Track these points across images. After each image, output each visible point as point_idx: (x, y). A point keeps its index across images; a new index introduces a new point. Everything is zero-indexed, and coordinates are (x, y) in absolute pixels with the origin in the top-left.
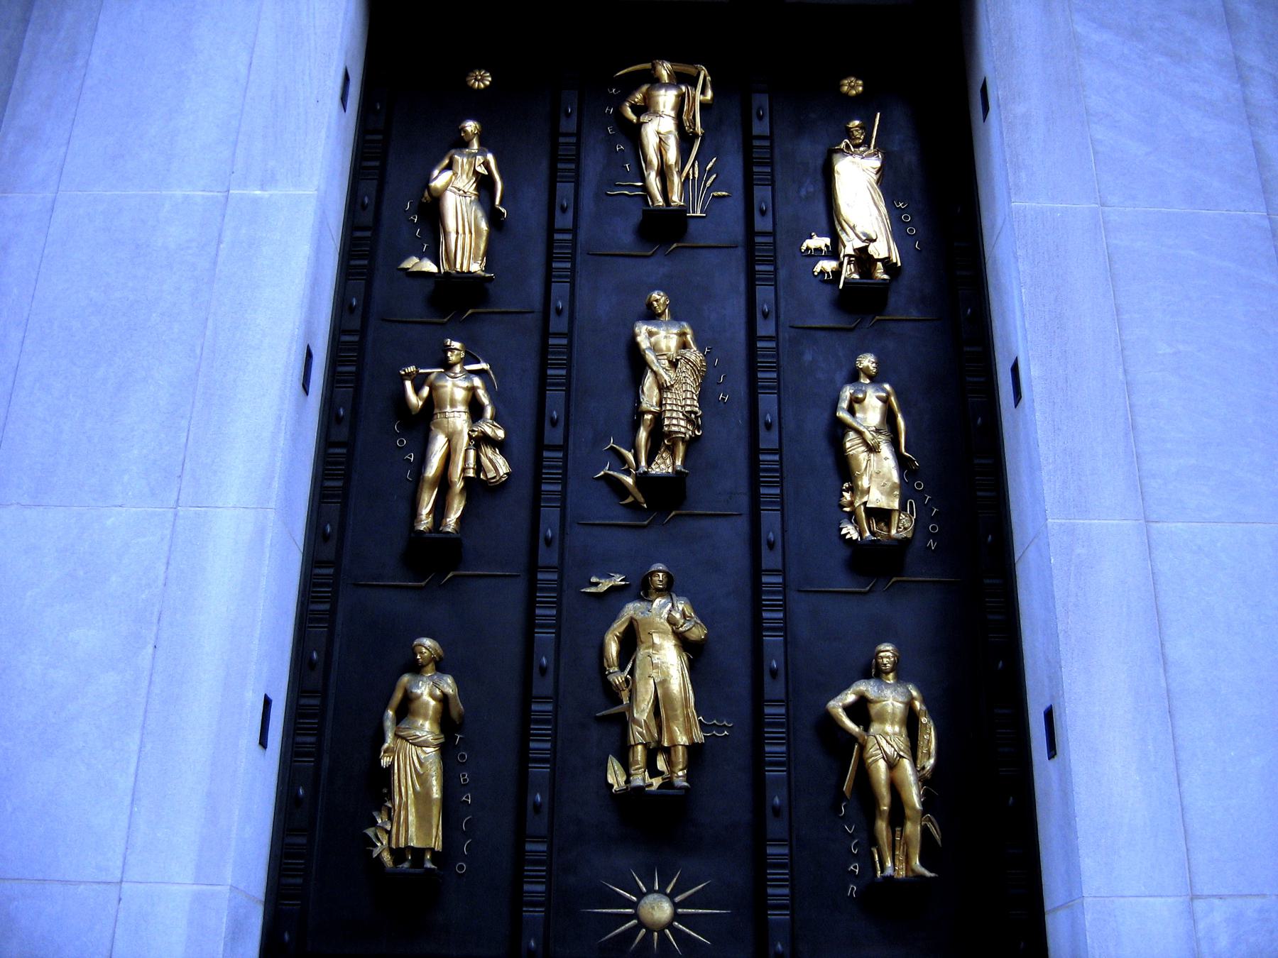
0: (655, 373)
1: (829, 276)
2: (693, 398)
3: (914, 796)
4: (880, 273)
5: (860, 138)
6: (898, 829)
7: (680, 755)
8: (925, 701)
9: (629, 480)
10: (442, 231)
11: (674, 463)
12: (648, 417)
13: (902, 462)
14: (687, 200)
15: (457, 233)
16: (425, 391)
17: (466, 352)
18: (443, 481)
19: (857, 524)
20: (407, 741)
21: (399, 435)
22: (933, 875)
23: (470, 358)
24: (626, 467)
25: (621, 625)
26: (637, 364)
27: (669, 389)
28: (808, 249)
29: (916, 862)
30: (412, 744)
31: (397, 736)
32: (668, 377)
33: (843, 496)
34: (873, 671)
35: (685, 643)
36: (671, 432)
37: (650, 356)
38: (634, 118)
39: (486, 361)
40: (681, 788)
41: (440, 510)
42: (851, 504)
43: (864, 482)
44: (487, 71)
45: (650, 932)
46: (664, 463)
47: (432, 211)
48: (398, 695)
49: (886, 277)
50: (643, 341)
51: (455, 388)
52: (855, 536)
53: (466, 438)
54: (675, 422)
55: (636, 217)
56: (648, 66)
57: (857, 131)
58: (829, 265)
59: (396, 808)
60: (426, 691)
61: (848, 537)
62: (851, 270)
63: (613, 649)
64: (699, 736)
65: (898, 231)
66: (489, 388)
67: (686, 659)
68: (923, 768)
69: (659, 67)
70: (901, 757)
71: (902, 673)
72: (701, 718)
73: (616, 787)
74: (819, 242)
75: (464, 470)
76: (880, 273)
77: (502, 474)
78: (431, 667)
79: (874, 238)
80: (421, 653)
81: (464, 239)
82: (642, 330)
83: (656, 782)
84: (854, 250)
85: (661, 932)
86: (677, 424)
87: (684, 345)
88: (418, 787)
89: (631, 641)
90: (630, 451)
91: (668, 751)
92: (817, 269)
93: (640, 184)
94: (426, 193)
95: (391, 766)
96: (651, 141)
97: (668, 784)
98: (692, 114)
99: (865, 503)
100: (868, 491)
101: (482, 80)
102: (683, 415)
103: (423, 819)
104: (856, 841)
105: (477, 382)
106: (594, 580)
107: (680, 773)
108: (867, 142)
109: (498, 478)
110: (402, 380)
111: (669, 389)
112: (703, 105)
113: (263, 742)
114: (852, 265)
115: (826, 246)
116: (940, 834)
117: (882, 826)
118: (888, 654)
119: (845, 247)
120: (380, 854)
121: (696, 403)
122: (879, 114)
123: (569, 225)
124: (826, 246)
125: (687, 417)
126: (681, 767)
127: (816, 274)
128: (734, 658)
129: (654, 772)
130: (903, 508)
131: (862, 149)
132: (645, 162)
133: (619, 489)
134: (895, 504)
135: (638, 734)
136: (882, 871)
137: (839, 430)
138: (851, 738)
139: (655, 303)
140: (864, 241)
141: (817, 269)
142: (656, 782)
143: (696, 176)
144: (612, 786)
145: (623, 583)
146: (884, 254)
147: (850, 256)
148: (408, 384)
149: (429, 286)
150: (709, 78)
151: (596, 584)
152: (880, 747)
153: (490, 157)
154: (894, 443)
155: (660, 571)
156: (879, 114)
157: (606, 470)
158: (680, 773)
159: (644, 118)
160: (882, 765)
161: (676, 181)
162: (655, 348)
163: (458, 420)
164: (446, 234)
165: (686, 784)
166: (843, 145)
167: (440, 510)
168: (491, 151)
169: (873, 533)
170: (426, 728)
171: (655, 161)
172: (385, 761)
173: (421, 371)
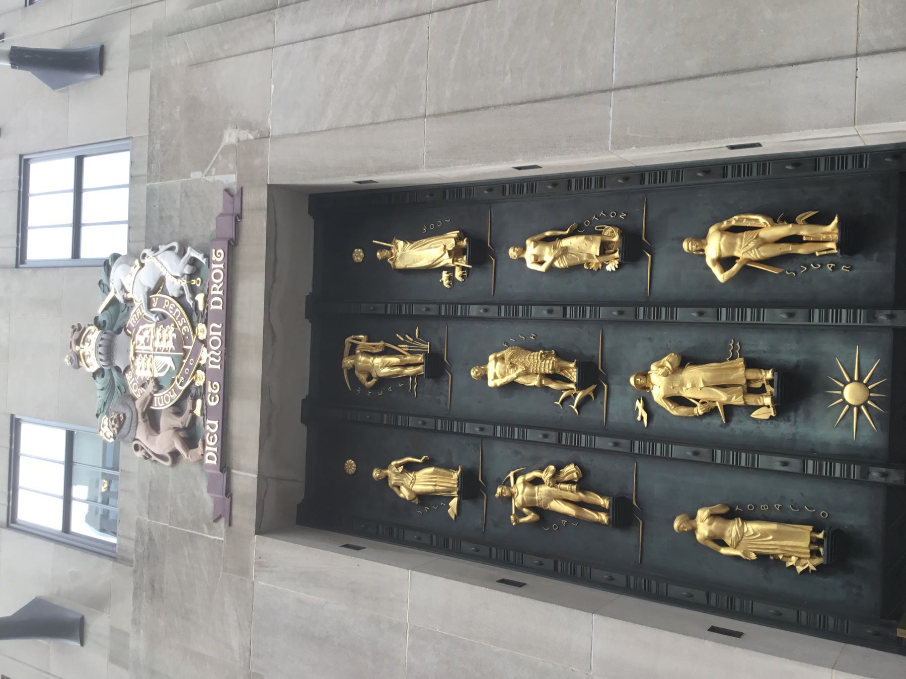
1: (465, 273)
2: (533, 355)
3: (783, 230)
5: (387, 253)
6: (804, 239)
7: (752, 374)
10: (434, 494)
13: (573, 234)
14: (420, 353)
15: (435, 485)
16: (525, 510)
17: (503, 485)
18: (580, 504)
20: (739, 541)
21: (551, 528)
22: (836, 218)
23: (507, 483)
25: (668, 405)
26: (512, 386)
27: (527, 369)
28: (449, 284)
30: (742, 537)
33: (592, 269)
34: (702, 253)
36: (553, 369)
37: (508, 378)
38: (374, 380)
39: (509, 473)
40: (773, 375)
41: (597, 508)
44: (345, 462)
45: (870, 398)
47: (424, 498)
48: (712, 545)
49: (465, 240)
50: (499, 382)
52: (617, 262)
53: (552, 489)
54: (547, 367)
55: (429, 383)
56: (345, 371)
57: (383, 254)
58: (458, 273)
59: (782, 552)
61: (617, 267)
62: (461, 260)
63: (682, 411)
64: (740, 362)
65: (439, 232)
66: (523, 473)
67: (689, 367)
69: (346, 365)
70: (757, 236)
71: (702, 237)
72: (728, 359)
74: (445, 275)
75: (572, 492)
76: (464, 243)
77: (575, 469)
78: (692, 522)
79: (443, 246)
80: (683, 527)
81: (439, 482)
83: (769, 389)
84: (450, 258)
85: (871, 391)
86: (548, 365)
87: (502, 358)
88: (771, 537)
90: (563, 393)
91: (748, 381)
94: (413, 501)
95: (755, 553)
96: (385, 371)
98: (372, 347)
99: (597, 256)
101: (351, 466)
102: (543, 361)
103: (790, 536)
104: (812, 265)
105: (520, 480)
106: (639, 418)
107: (764, 374)
108: (389, 249)
109: (577, 471)
110: (519, 525)
111: (527, 369)
112: (368, 341)
113: (738, 635)
114: (459, 259)
115: (447, 273)
116: (808, 213)
117: (802, 250)
119: (448, 264)
120: (814, 566)
121: (536, 353)
122: (374, 241)
123: (433, 421)
124: (447, 273)
125: (544, 359)
126: (759, 374)
127: (463, 280)
129: (761, 391)
130: (600, 233)
131: (393, 251)
132: (399, 375)
134: (598, 239)
135: (737, 400)
138: (745, 268)
139: (478, 375)
140: (445, 253)
141: (460, 279)
142: (769, 389)
144: (771, 417)
145: (641, 401)
146: (453, 241)
149: (467, 504)
151: (642, 418)
153: (393, 463)
154: (562, 237)
155: (635, 380)
156: (374, 241)
157: (574, 407)
158: (764, 374)
159: (374, 375)
161: (409, 358)
163: (542, 491)
164: (436, 491)
165: (770, 371)
166: (391, 262)
167: (597, 508)
168: (390, 463)
169: (615, 252)
170: (733, 529)
171: (398, 369)
173: (513, 512)
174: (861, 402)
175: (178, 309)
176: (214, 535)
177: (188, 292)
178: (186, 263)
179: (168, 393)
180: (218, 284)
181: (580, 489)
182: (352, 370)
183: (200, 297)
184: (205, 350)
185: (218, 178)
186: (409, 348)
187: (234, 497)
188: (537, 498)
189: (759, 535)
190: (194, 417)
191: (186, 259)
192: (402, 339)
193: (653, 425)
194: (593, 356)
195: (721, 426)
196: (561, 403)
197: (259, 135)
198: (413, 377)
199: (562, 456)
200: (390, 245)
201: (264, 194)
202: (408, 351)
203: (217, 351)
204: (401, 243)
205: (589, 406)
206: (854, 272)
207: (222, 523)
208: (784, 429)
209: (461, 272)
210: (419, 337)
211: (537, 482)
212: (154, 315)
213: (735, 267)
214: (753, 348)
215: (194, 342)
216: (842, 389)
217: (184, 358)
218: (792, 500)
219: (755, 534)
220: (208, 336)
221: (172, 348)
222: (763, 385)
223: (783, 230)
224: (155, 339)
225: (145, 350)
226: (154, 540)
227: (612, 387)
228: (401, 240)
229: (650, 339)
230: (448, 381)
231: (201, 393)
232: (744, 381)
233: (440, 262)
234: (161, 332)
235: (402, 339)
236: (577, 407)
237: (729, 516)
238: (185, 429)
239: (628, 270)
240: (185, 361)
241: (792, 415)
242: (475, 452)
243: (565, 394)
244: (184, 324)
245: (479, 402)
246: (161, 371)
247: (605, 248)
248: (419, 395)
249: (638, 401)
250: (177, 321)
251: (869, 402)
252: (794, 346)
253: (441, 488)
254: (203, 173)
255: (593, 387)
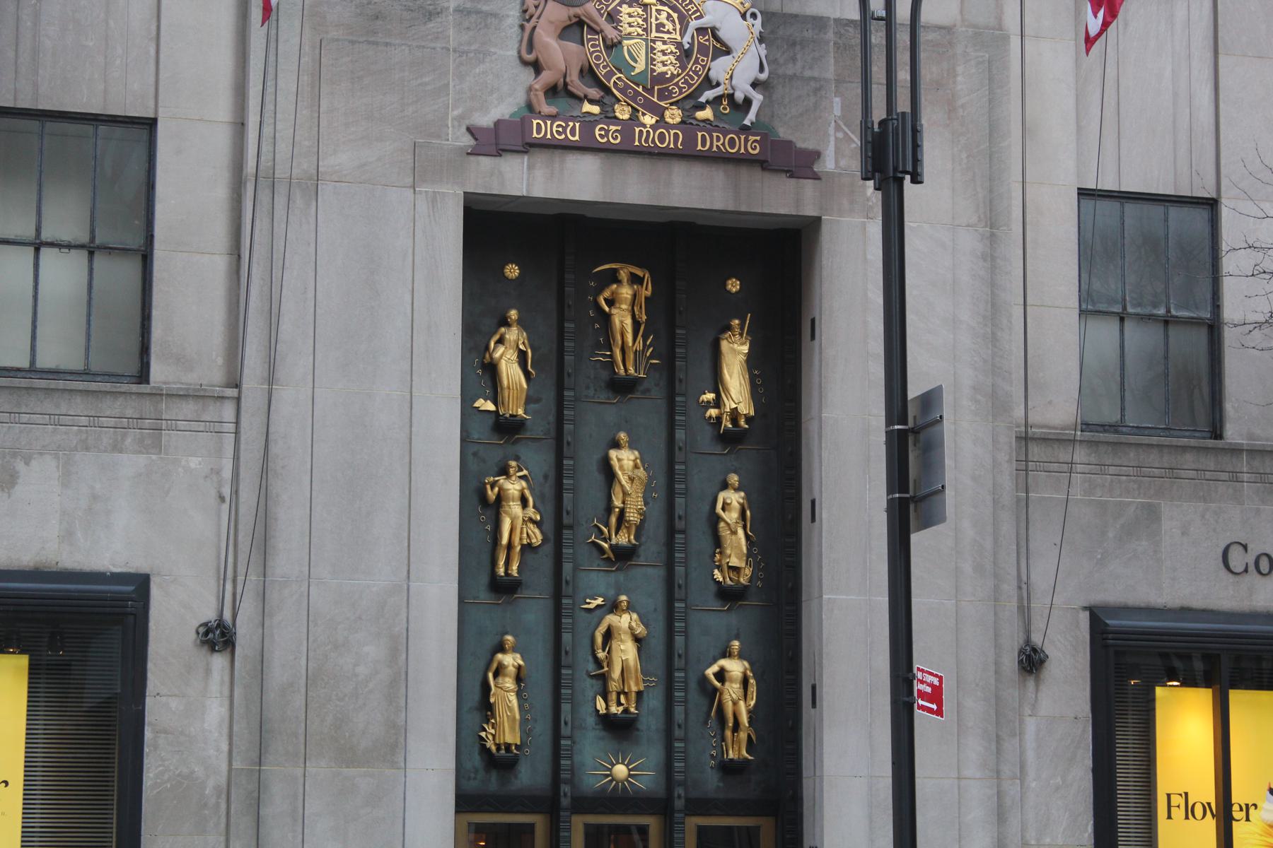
0: (622, 486)
3: (744, 719)
4: (742, 422)
7: (633, 696)
8: (752, 671)
9: (606, 545)
11: (629, 537)
12: (617, 510)
16: (496, 489)
18: (510, 546)
19: (721, 571)
21: (482, 515)
24: (603, 537)
26: (609, 474)
28: (703, 401)
29: (744, 753)
31: (495, 686)
32: (628, 487)
34: (728, 655)
35: (637, 640)
39: (527, 469)
42: (720, 561)
43: (728, 552)
44: (519, 269)
45: (617, 783)
46: (624, 535)
48: (495, 666)
49: (747, 426)
50: (615, 463)
51: (513, 487)
52: (721, 579)
54: (632, 515)
55: (605, 375)
58: (713, 412)
60: (510, 660)
63: (599, 640)
68: (750, 705)
71: (741, 656)
73: (601, 712)
74: (710, 396)
75: (521, 539)
76: (742, 422)
81: (513, 393)
82: (613, 454)
83: (621, 709)
84: (731, 409)
85: (623, 784)
86: (633, 516)
88: (509, 714)
89: (609, 635)
91: (626, 694)
92: (708, 414)
93: (609, 353)
97: (626, 711)
99: (728, 562)
100: (730, 556)
103: (512, 729)
105: (524, 484)
106: (588, 601)
110: (485, 484)
112: (646, 298)
117: (728, 733)
118: (737, 647)
124: (713, 399)
128: (657, 645)
129: (619, 704)
133: (601, 550)
134: (743, 565)
136: (727, 756)
137: (715, 520)
138: (715, 690)
141: (708, 414)
143: (641, 348)
144: (599, 711)
147: (727, 412)
148: (488, 487)
149: (490, 421)
150: (649, 279)
151: (589, 603)
152: (730, 695)
154: (744, 528)
160: (730, 703)
162: (621, 468)
163: (516, 508)
166: (727, 335)
170: (509, 683)
172: (492, 700)
174: (614, 776)
175: (698, 80)
176: (453, 126)
177: (715, 95)
178: (747, 94)
179: (604, 60)
180: (723, 144)
181: (523, 546)
182: (613, 277)
183: (707, 113)
184: (653, 121)
185: (832, 139)
186: (639, 351)
187: (497, 159)
188: (511, 503)
189: (510, 705)
190: (580, 100)
191: (750, 94)
192: (648, 343)
193: (583, 613)
194: (639, 556)
195: (587, 671)
196: (596, 525)
197: (870, 203)
198: (611, 356)
199: (549, 526)
200: (745, 335)
201: (810, 211)
202: (636, 350)
203: (653, 141)
204: (745, 349)
205: (595, 553)
206: (709, 770)
207: (467, 141)
208: (591, 721)
209: (714, 415)
210: (651, 363)
211: (524, 502)
212: (690, 41)
213: (718, 684)
214: (651, 695)
215: (662, 103)
216: (623, 763)
217: (644, 88)
218: (534, 728)
219: (510, 701)
220: (669, 127)
221: (655, 71)
222: (623, 705)
223: (744, 719)
224: (664, 43)
225: (651, 23)
226: (430, 20)
227: (613, 574)
228: (749, 350)
229: (655, 610)
230: (609, 399)
231: (607, 111)
232: (626, 690)
233: (728, 399)
234: (672, 52)
235: (648, 343)
236: (593, 542)
237: (519, 679)
238: (566, 84)
239: (713, 588)
240: (640, 90)
241: (600, 727)
242: (542, 431)
243: (605, 530)
244: (680, 89)
245: (591, 436)
246: (629, 52)
247: (736, 569)
248: (593, 363)
249: (602, 599)
250: (684, 77)
251: (614, 782)
252: (653, 727)
253: (506, 395)
254: (839, 117)
255: (612, 556)
